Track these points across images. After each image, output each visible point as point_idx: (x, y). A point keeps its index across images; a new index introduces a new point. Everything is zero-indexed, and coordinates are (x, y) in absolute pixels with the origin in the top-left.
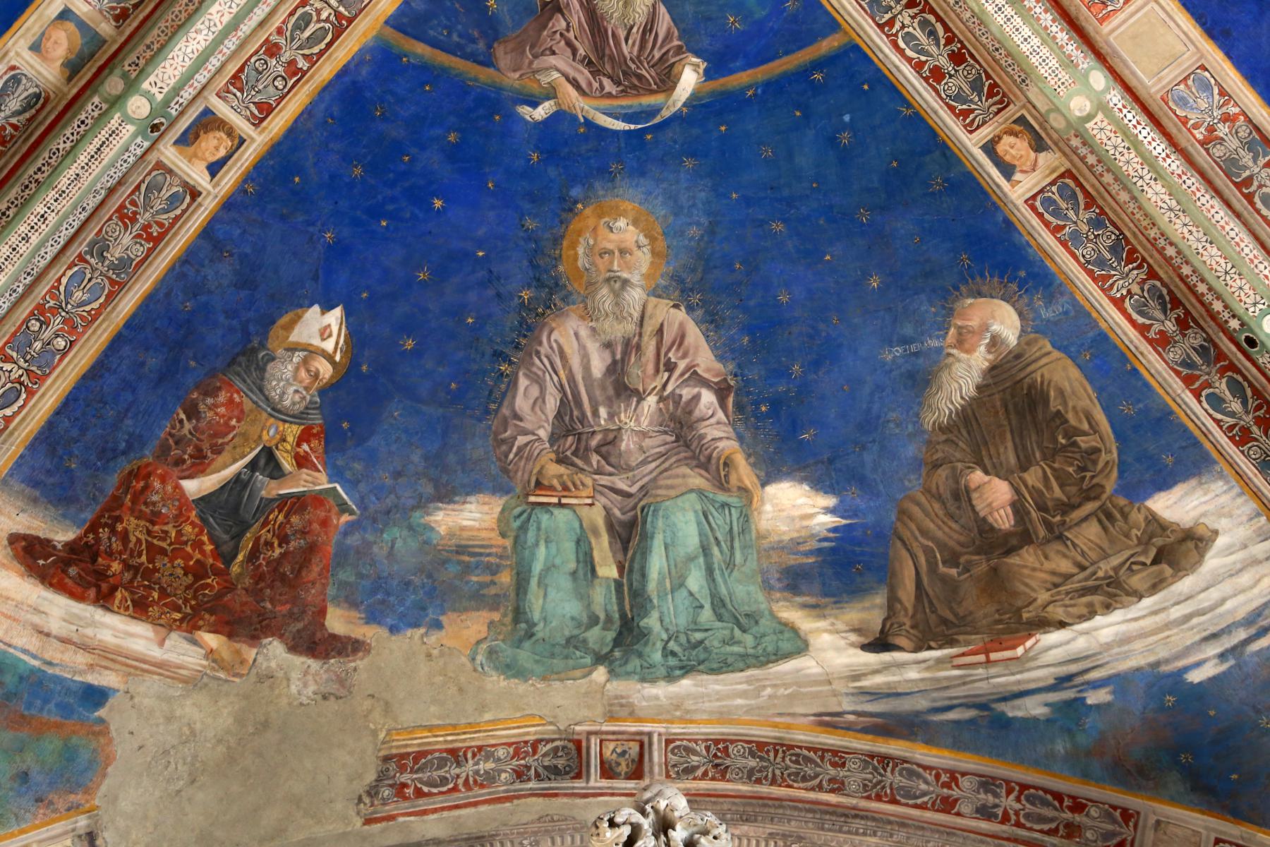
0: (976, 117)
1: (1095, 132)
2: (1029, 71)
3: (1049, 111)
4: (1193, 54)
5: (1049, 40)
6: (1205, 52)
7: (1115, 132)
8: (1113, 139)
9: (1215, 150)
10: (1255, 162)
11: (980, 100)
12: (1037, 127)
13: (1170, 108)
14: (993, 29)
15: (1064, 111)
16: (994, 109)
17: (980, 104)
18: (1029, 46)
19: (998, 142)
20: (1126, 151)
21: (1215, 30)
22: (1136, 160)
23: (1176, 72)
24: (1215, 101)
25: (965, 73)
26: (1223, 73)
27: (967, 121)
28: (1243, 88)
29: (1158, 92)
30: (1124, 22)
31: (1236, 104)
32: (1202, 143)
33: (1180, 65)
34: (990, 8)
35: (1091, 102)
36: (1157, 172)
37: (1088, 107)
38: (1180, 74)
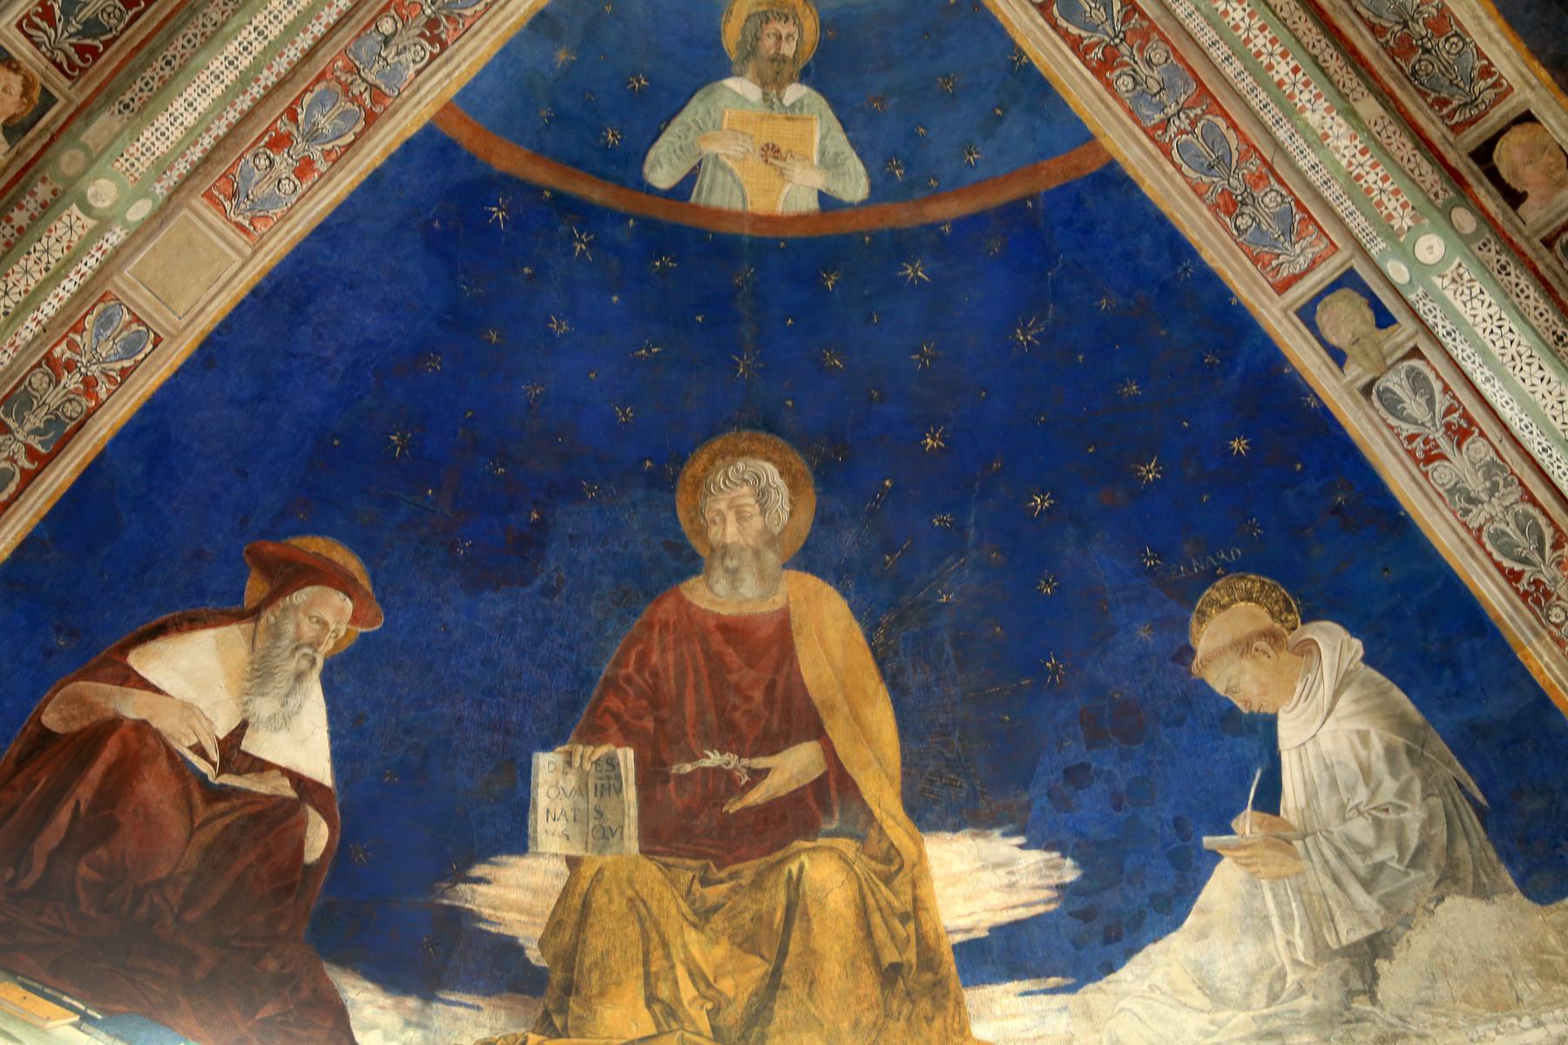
0: (45, 32)
1: (65, 219)
2: (145, 114)
3: (84, 147)
4: (175, 326)
5: (192, 136)
6: (179, 341)
7: (69, 247)
8: (59, 246)
9: (39, 376)
10: (31, 432)
11: (71, 36)
12: (40, 125)
13: (94, 306)
14: (201, 57)
15: (92, 172)
16: (60, 57)
17: (65, 36)
18: (182, 110)
19: (9, 68)
20: (43, 266)
21: (212, 350)
22: (32, 282)
23: (148, 309)
24: (112, 365)
25: (110, 10)
26: (153, 369)
27: (37, 20)
28: (136, 398)
29: (116, 286)
30: (211, 227)
31: (110, 394)
32: (48, 358)
33: (157, 310)
34: (231, 48)
35: (111, 208)
36: (17, 314)
37: (102, 204)
38: (144, 311)
